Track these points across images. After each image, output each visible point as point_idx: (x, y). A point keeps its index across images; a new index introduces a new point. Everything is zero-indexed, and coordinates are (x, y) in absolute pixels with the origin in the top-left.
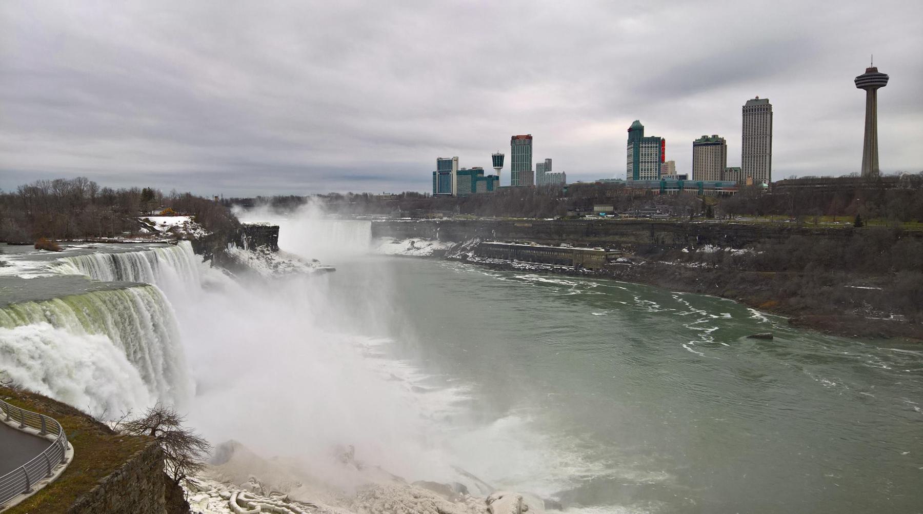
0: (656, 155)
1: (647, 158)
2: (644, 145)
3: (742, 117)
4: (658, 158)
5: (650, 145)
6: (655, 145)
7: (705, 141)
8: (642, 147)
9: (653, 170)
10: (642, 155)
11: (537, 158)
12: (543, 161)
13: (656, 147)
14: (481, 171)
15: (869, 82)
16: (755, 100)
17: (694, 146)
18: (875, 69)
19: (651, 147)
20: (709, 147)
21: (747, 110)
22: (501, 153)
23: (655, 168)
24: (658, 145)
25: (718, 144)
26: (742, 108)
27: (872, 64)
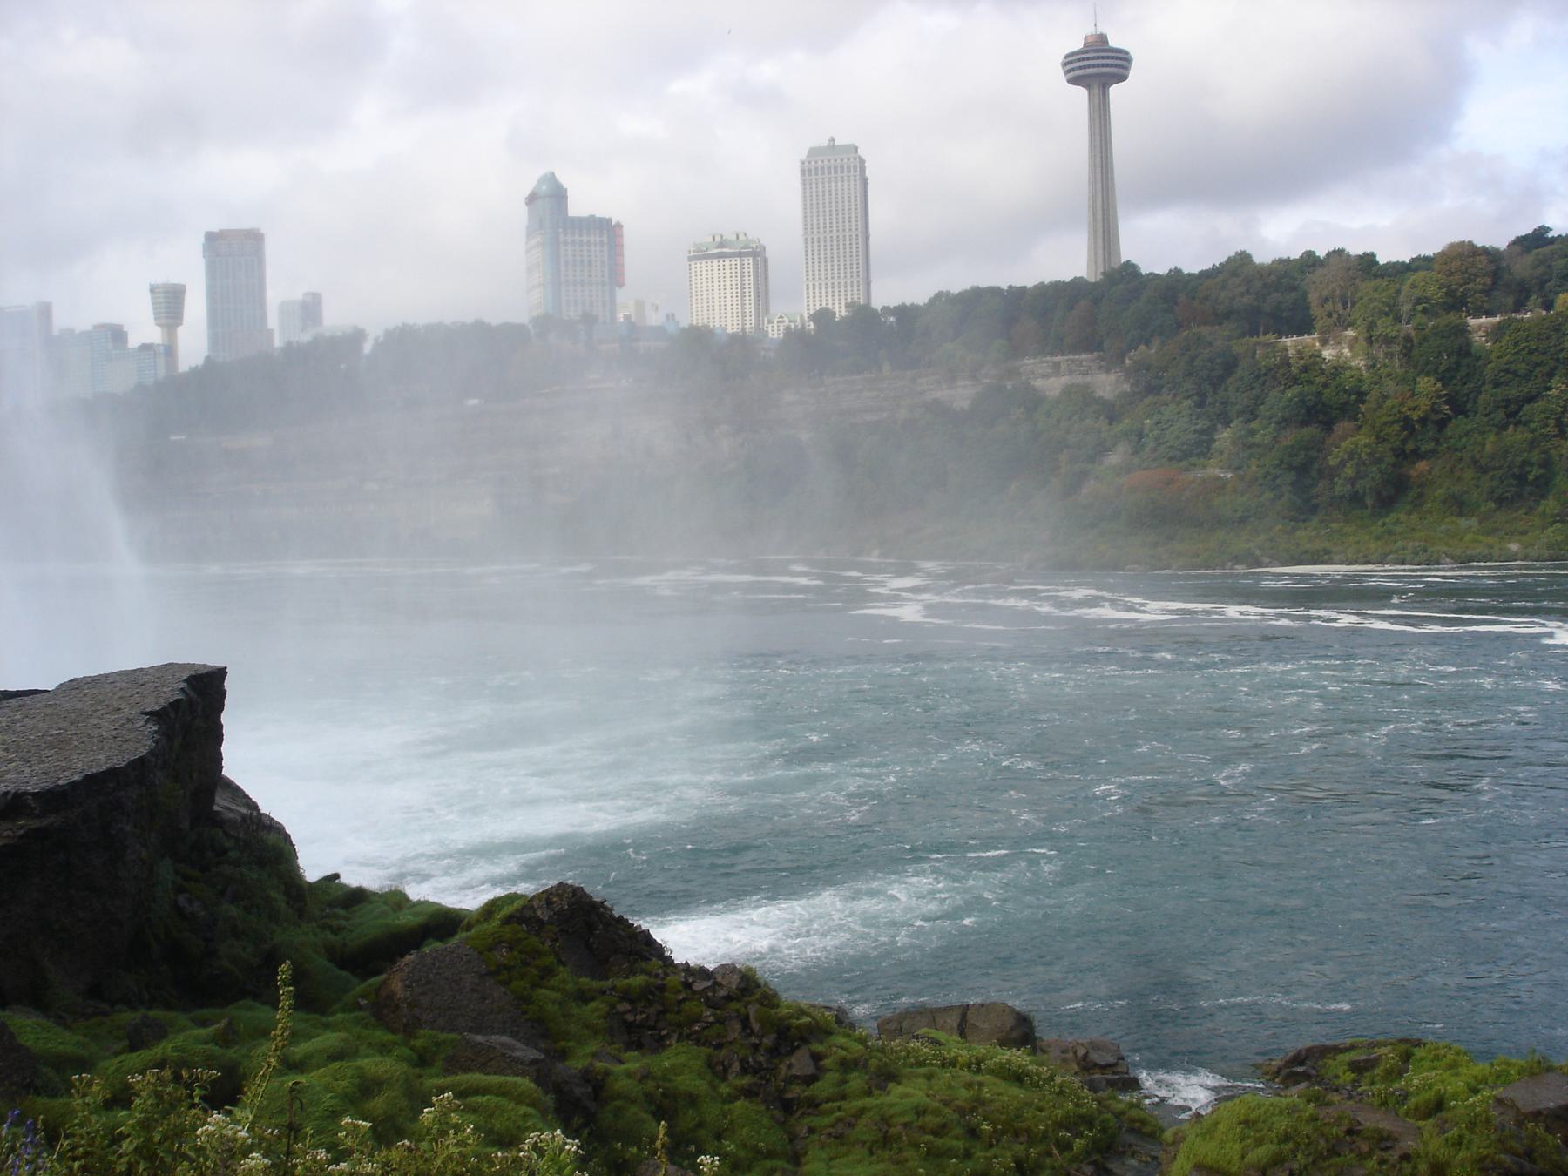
2: (569, 238)
5: (585, 238)
6: (598, 239)
7: (717, 248)
11: (281, 289)
12: (298, 295)
14: (117, 334)
15: (1094, 66)
16: (829, 146)
17: (691, 259)
18: (1102, 39)
19: (589, 241)
20: (727, 260)
21: (810, 170)
22: (175, 279)
24: (605, 239)
25: (747, 254)
26: (799, 164)
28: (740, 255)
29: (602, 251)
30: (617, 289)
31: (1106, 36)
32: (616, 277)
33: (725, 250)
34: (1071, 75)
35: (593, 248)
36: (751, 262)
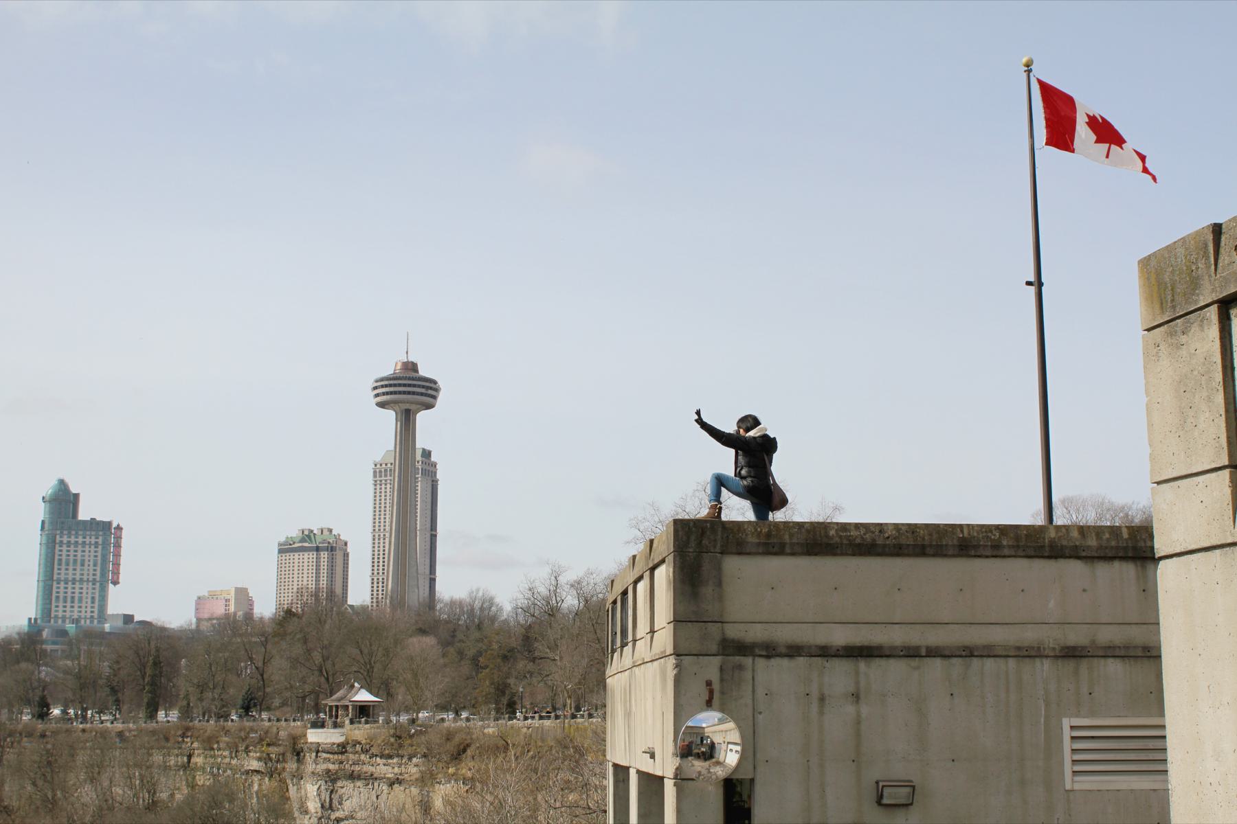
0: (95, 565)
1: (71, 572)
3: (372, 487)
4: (98, 573)
5: (80, 540)
6: (93, 540)
7: (300, 542)
8: (61, 542)
9: (84, 600)
10: (60, 564)
13: (96, 545)
17: (281, 551)
18: (411, 367)
20: (306, 554)
21: (380, 472)
23: (90, 596)
24: (100, 540)
27: (407, 353)
28: (318, 549)
29: (96, 552)
30: (111, 586)
31: (416, 364)
32: (108, 573)
33: (306, 545)
34: (379, 399)
35: (87, 548)
36: (326, 556)
